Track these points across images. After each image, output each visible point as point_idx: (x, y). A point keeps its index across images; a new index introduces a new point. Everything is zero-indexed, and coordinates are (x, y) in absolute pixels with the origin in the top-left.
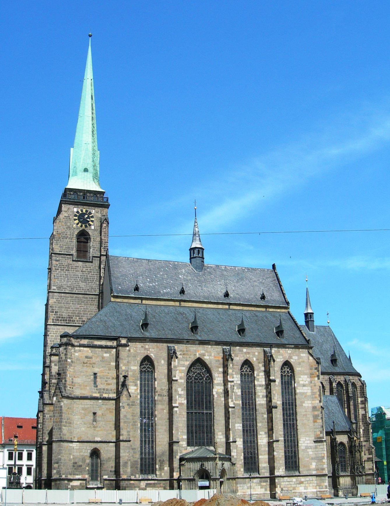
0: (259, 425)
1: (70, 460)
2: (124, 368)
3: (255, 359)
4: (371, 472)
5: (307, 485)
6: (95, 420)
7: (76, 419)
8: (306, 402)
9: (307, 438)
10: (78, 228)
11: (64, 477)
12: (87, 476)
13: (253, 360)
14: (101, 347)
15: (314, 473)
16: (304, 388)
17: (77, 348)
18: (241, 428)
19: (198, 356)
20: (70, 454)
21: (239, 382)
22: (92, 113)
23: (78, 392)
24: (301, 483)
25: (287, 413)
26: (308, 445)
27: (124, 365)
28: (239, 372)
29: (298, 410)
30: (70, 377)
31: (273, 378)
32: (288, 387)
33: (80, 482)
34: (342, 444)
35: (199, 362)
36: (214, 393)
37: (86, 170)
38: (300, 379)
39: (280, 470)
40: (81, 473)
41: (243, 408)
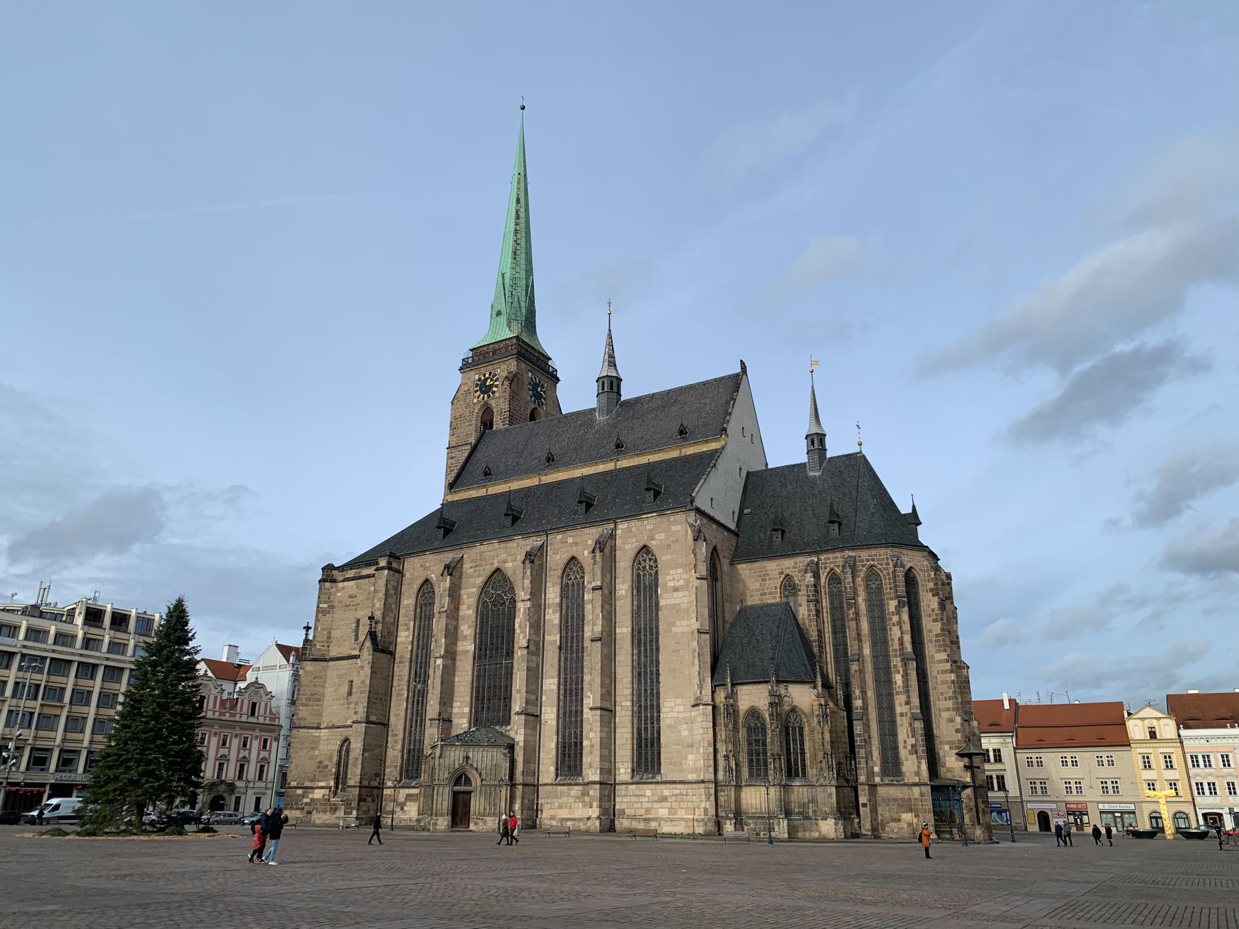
0: (587, 678)
1: (312, 758)
2: (377, 605)
3: (586, 553)
4: (917, 780)
5: (675, 805)
6: (350, 693)
7: (329, 690)
8: (678, 623)
9: (679, 701)
10: (479, 402)
11: (294, 784)
12: (332, 783)
13: (585, 555)
14: (368, 576)
15: (691, 777)
16: (676, 594)
17: (340, 585)
18: (555, 687)
19: (496, 565)
20: (312, 748)
21: (558, 600)
22: (517, 224)
23: (334, 652)
24: (664, 799)
25: (646, 651)
26: (682, 715)
27: (379, 600)
28: (559, 581)
29: (663, 642)
30: (323, 629)
31: (599, 583)
32: (651, 597)
33: (323, 791)
34: (753, 713)
35: (497, 579)
36: (517, 626)
37: (499, 313)
38: (668, 578)
39: (624, 771)
40: (325, 778)
41: (560, 648)
